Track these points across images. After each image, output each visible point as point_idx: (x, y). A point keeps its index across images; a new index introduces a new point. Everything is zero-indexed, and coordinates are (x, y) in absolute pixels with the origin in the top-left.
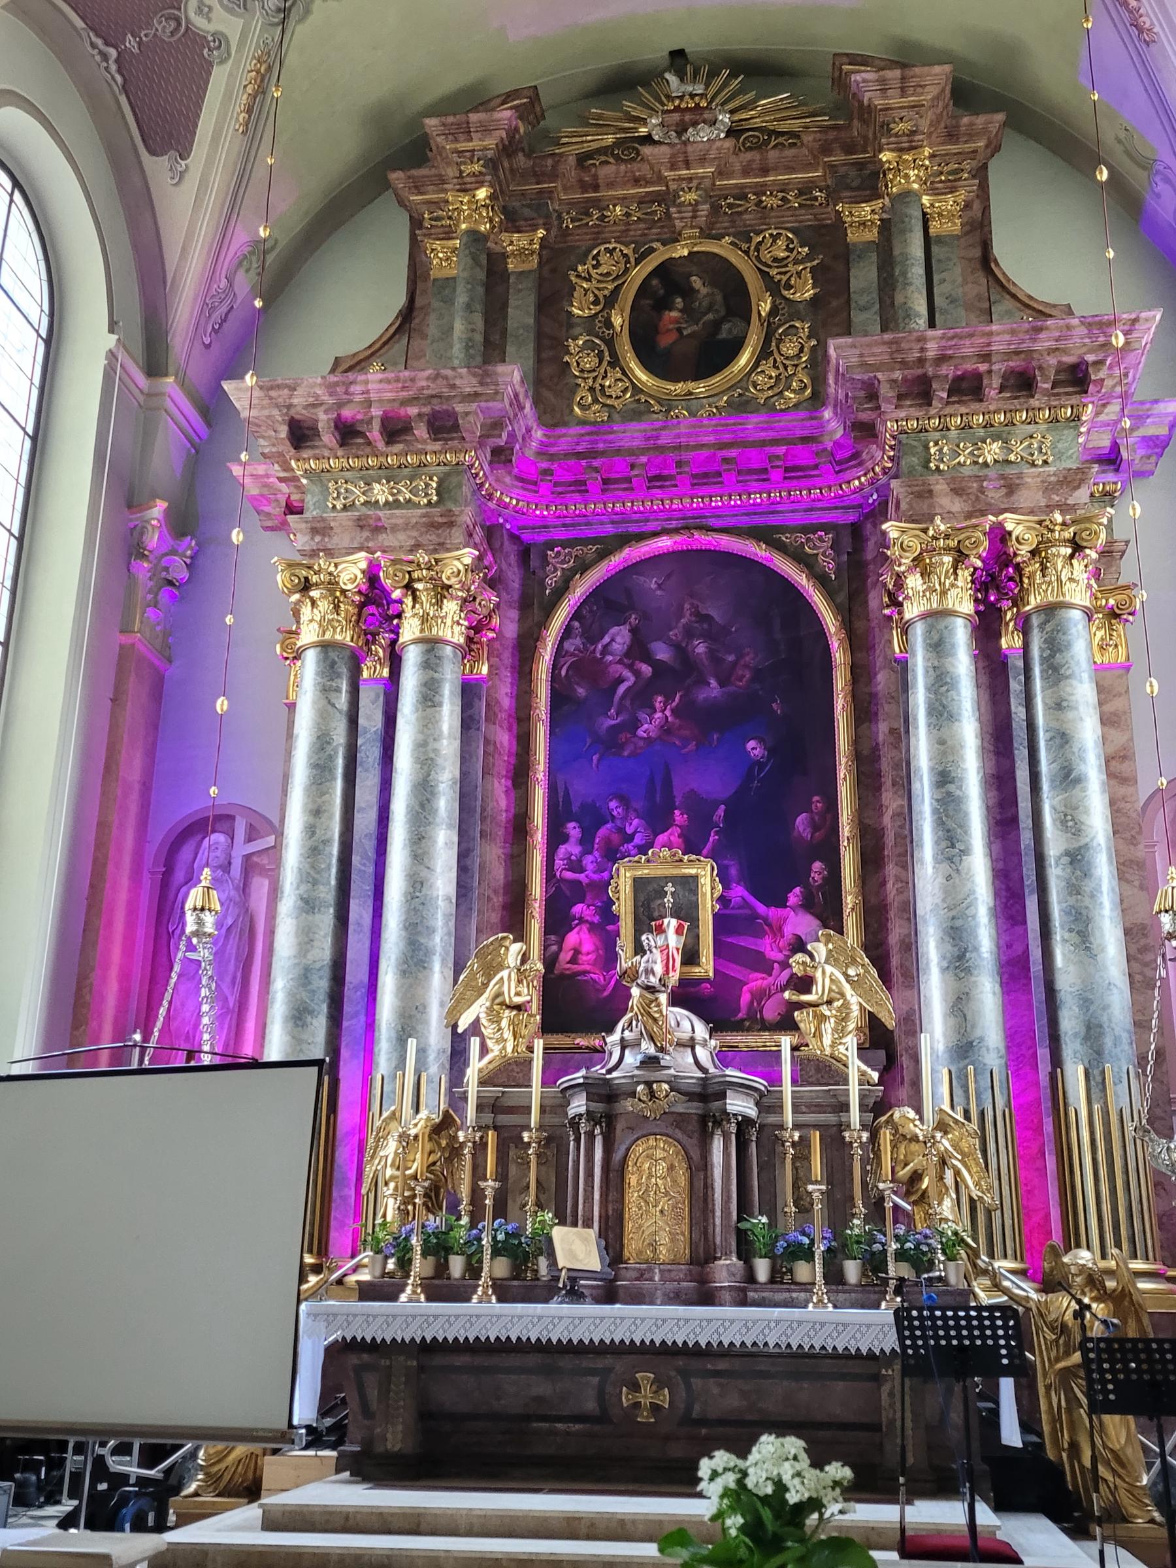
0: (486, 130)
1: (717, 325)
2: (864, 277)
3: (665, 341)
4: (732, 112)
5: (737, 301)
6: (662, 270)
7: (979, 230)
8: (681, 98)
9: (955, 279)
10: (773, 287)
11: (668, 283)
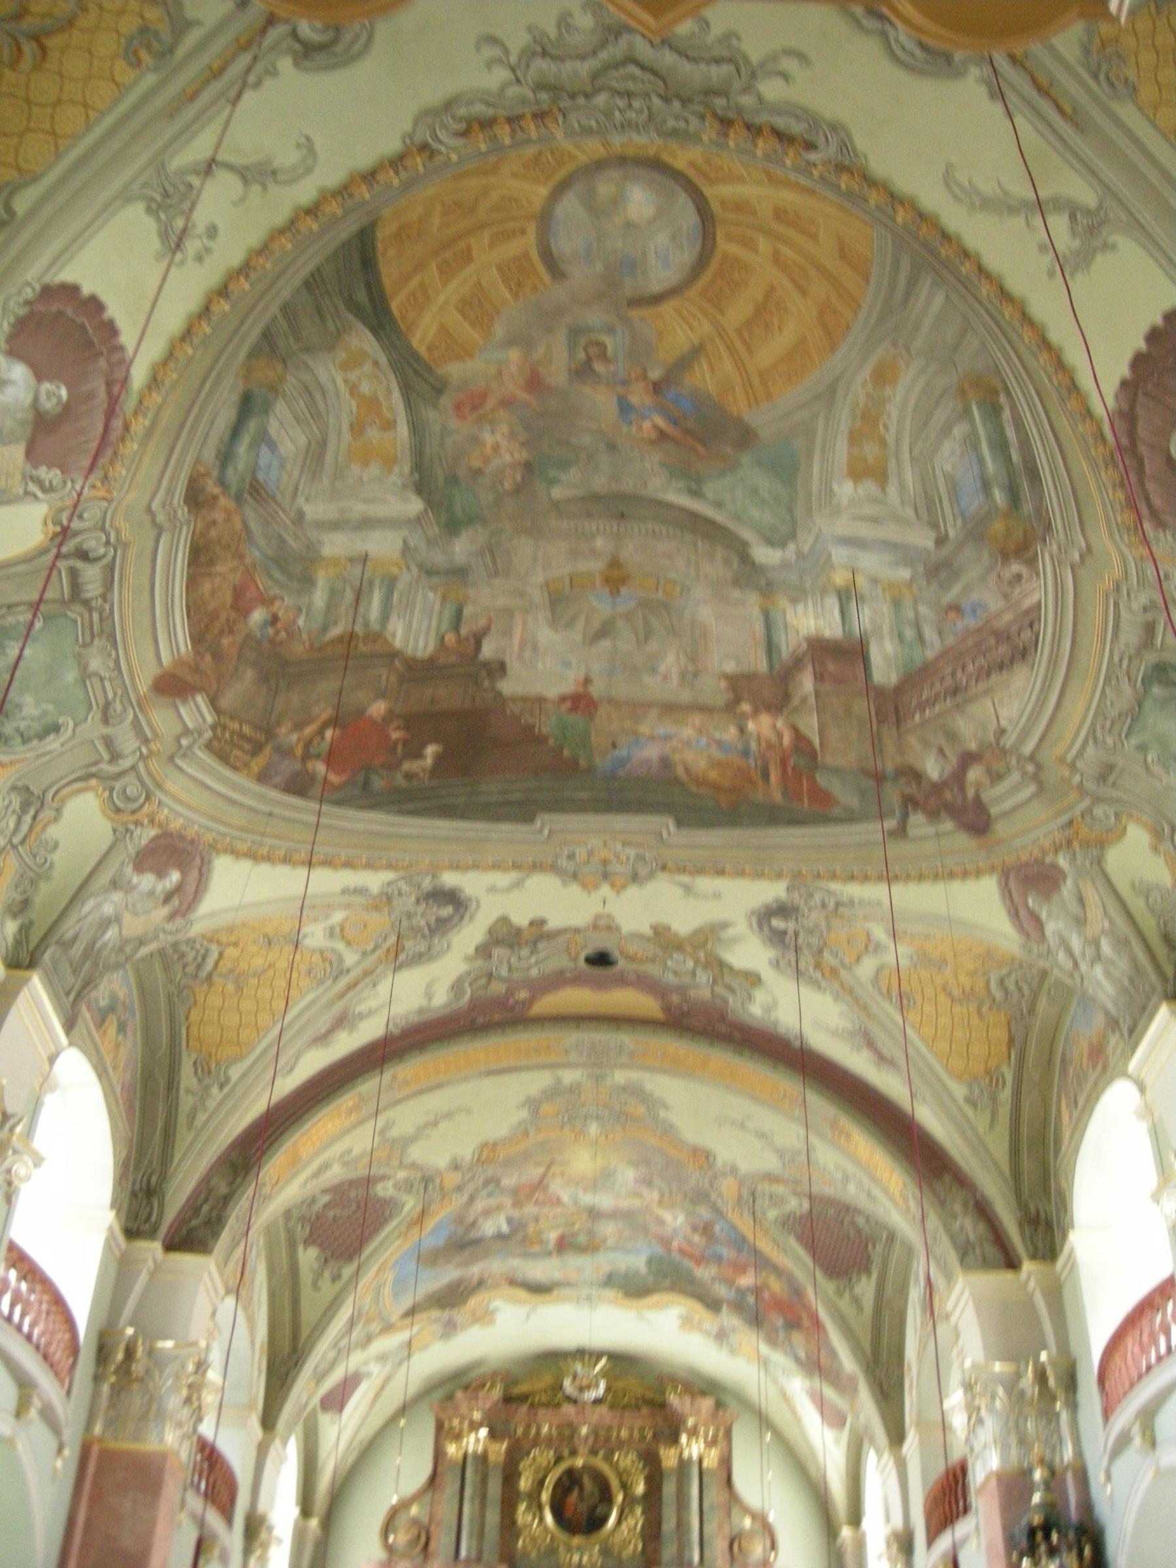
1: (594, 1508)
2: (669, 1489)
3: (568, 1514)
5: (606, 1497)
6: (570, 1473)
7: (726, 1462)
9: (715, 1495)
10: (625, 1486)
11: (570, 1481)
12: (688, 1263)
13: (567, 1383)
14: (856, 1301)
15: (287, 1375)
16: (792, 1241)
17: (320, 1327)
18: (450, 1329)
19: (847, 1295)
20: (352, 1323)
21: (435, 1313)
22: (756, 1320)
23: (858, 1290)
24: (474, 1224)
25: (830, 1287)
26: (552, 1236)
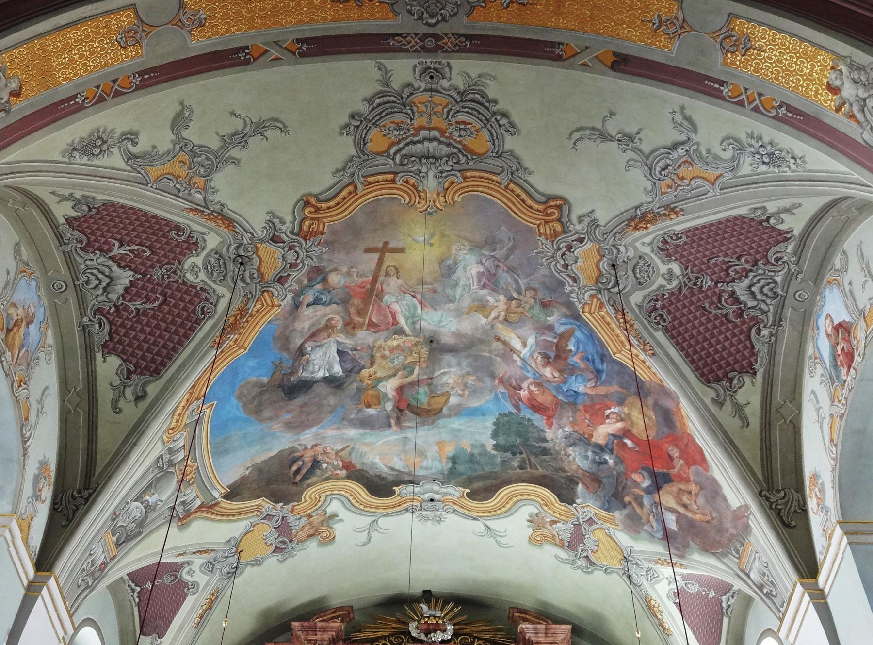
0: (324, 630)
4: (454, 625)
8: (428, 617)
12: (538, 420)
13: (412, 627)
14: (739, 409)
15: (74, 512)
16: (660, 336)
17: (119, 458)
18: (285, 540)
19: (728, 406)
20: (163, 469)
21: (266, 504)
22: (615, 496)
23: (741, 397)
24: (301, 352)
25: (708, 394)
26: (389, 387)
